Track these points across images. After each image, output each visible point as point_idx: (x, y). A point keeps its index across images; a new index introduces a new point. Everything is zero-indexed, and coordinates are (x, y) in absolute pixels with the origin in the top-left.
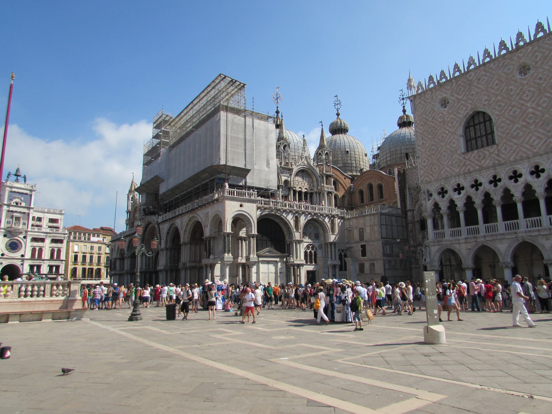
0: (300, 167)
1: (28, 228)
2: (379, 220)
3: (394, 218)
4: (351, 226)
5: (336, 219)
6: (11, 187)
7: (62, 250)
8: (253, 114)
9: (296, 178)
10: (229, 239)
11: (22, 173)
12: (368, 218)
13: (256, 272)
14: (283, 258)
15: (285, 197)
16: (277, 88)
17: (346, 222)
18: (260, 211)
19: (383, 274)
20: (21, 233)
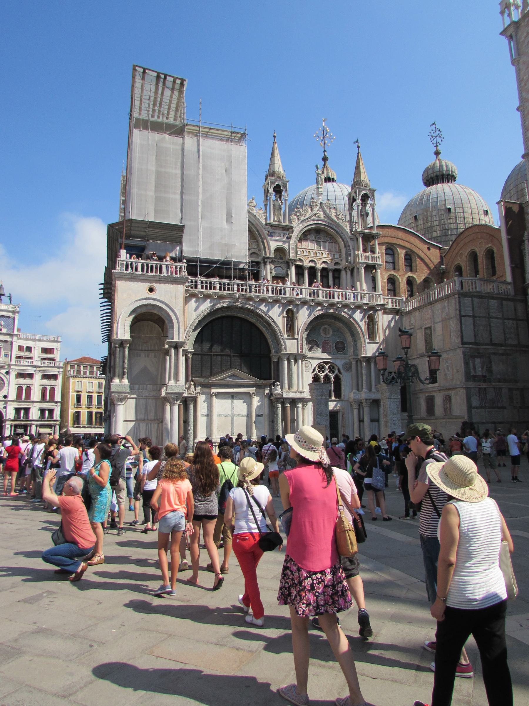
0: (309, 223)
1: (11, 361)
3: (494, 303)
5: (380, 313)
7: (56, 388)
9: (305, 244)
10: (124, 352)
12: (438, 306)
13: (206, 413)
14: (264, 387)
16: (324, 121)
17: (404, 319)
18: (211, 302)
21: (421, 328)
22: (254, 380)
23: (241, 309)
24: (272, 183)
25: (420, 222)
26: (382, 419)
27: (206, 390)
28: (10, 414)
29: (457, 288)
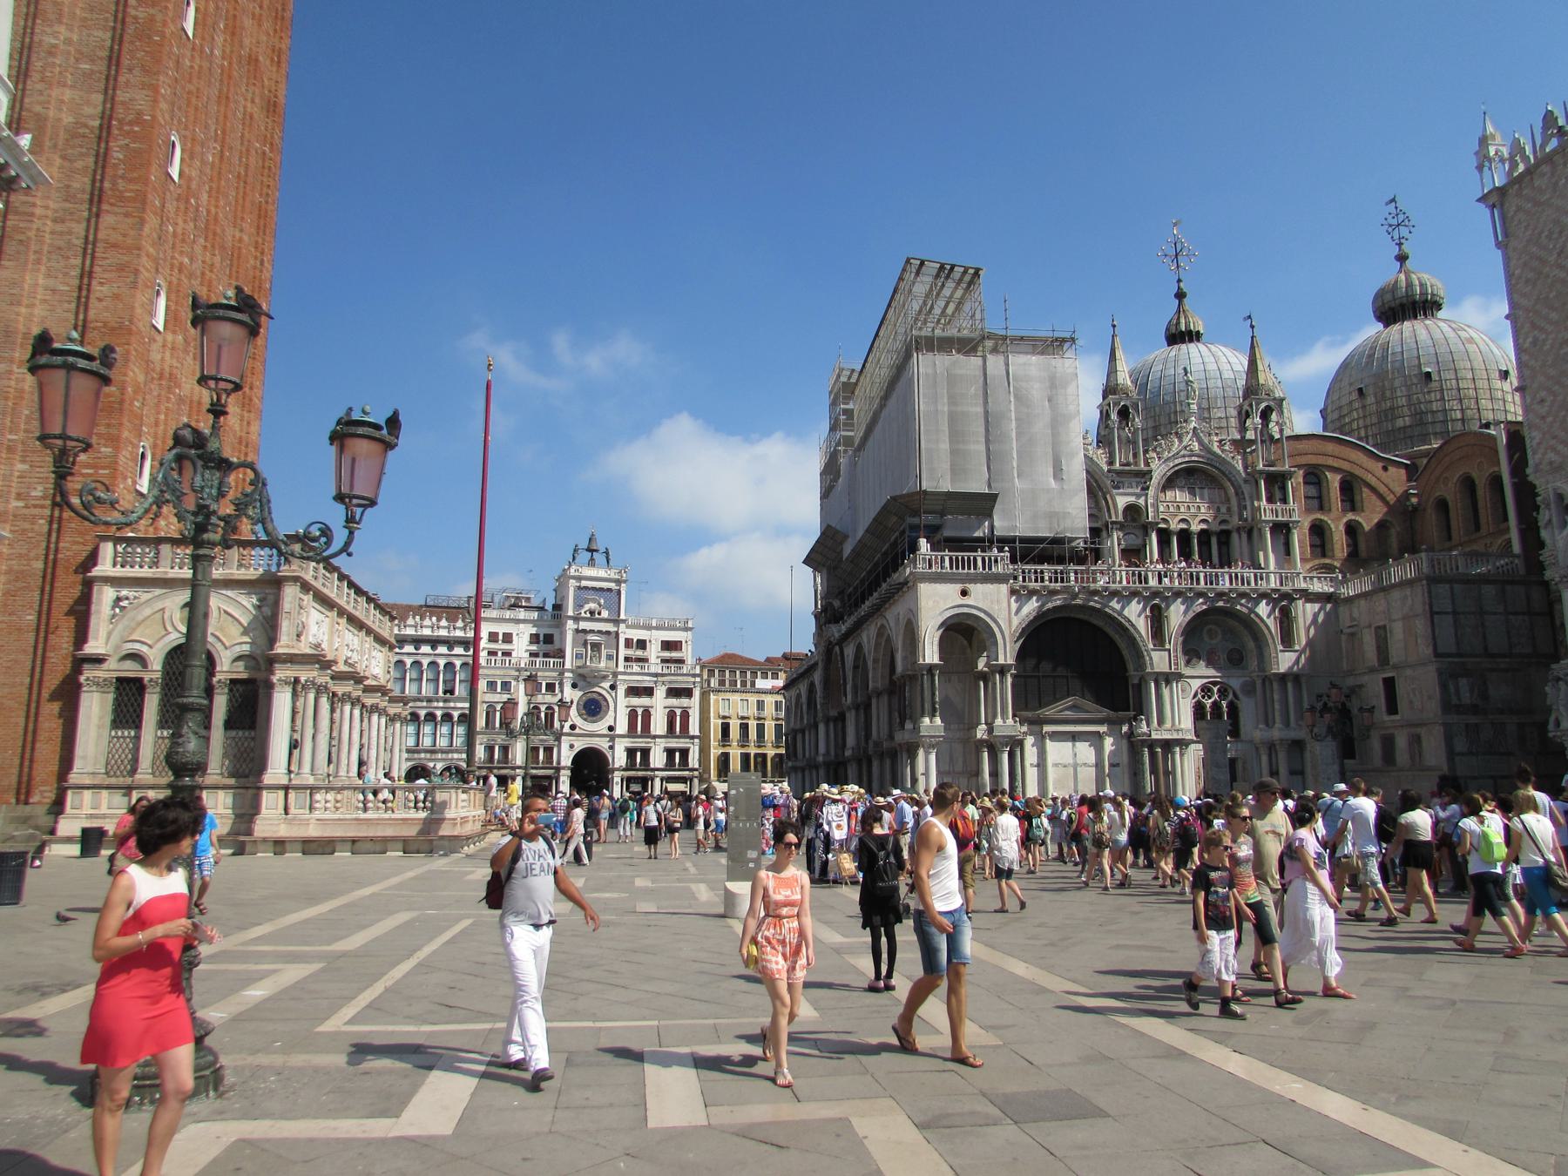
0: (1177, 462)
2: (1427, 600)
3: (1489, 591)
4: (1354, 620)
5: (1300, 603)
6: (579, 579)
7: (691, 712)
8: (1003, 343)
9: (1169, 494)
11: (600, 545)
12: (1396, 595)
14: (1121, 723)
15: (1133, 555)
16: (1175, 224)
17: (1341, 609)
18: (1037, 601)
19: (1445, 768)
20: (605, 678)
21: (1370, 626)
22: (1105, 712)
23: (1083, 608)
24: (1115, 404)
25: (1370, 400)
26: (1308, 770)
27: (1035, 728)
28: (619, 758)
29: (1425, 570)
